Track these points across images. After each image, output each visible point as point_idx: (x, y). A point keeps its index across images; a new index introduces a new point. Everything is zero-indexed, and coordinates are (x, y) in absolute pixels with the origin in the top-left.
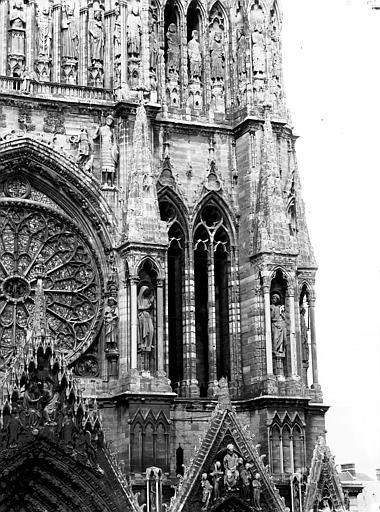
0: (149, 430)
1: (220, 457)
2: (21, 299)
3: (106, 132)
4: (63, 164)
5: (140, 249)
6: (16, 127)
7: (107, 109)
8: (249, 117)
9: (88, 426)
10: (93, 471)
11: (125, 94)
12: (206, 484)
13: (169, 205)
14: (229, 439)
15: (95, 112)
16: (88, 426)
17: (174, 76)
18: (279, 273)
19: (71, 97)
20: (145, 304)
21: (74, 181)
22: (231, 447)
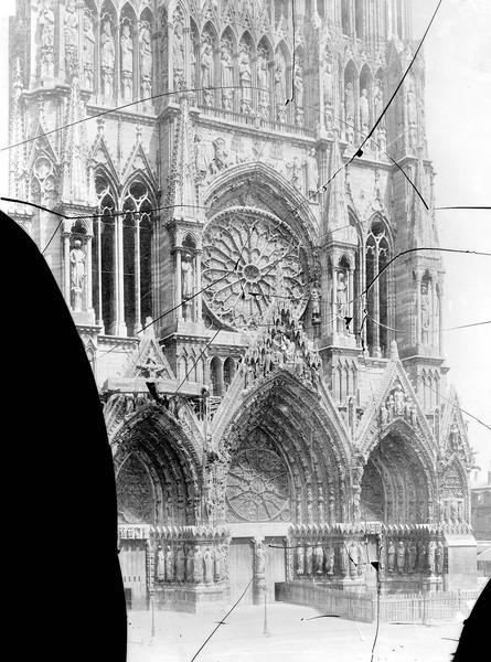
0: (343, 372)
1: (392, 392)
2: (255, 281)
3: (312, 162)
4: (283, 183)
5: (340, 247)
6: (251, 152)
7: (312, 145)
8: (408, 156)
9: (314, 365)
10: (316, 395)
11: (323, 134)
12: (384, 409)
13: (354, 220)
14: (398, 381)
15: (303, 145)
16: (314, 365)
17: (351, 123)
18: (427, 272)
19: (283, 133)
20: (342, 287)
21: (290, 198)
22: (399, 386)
